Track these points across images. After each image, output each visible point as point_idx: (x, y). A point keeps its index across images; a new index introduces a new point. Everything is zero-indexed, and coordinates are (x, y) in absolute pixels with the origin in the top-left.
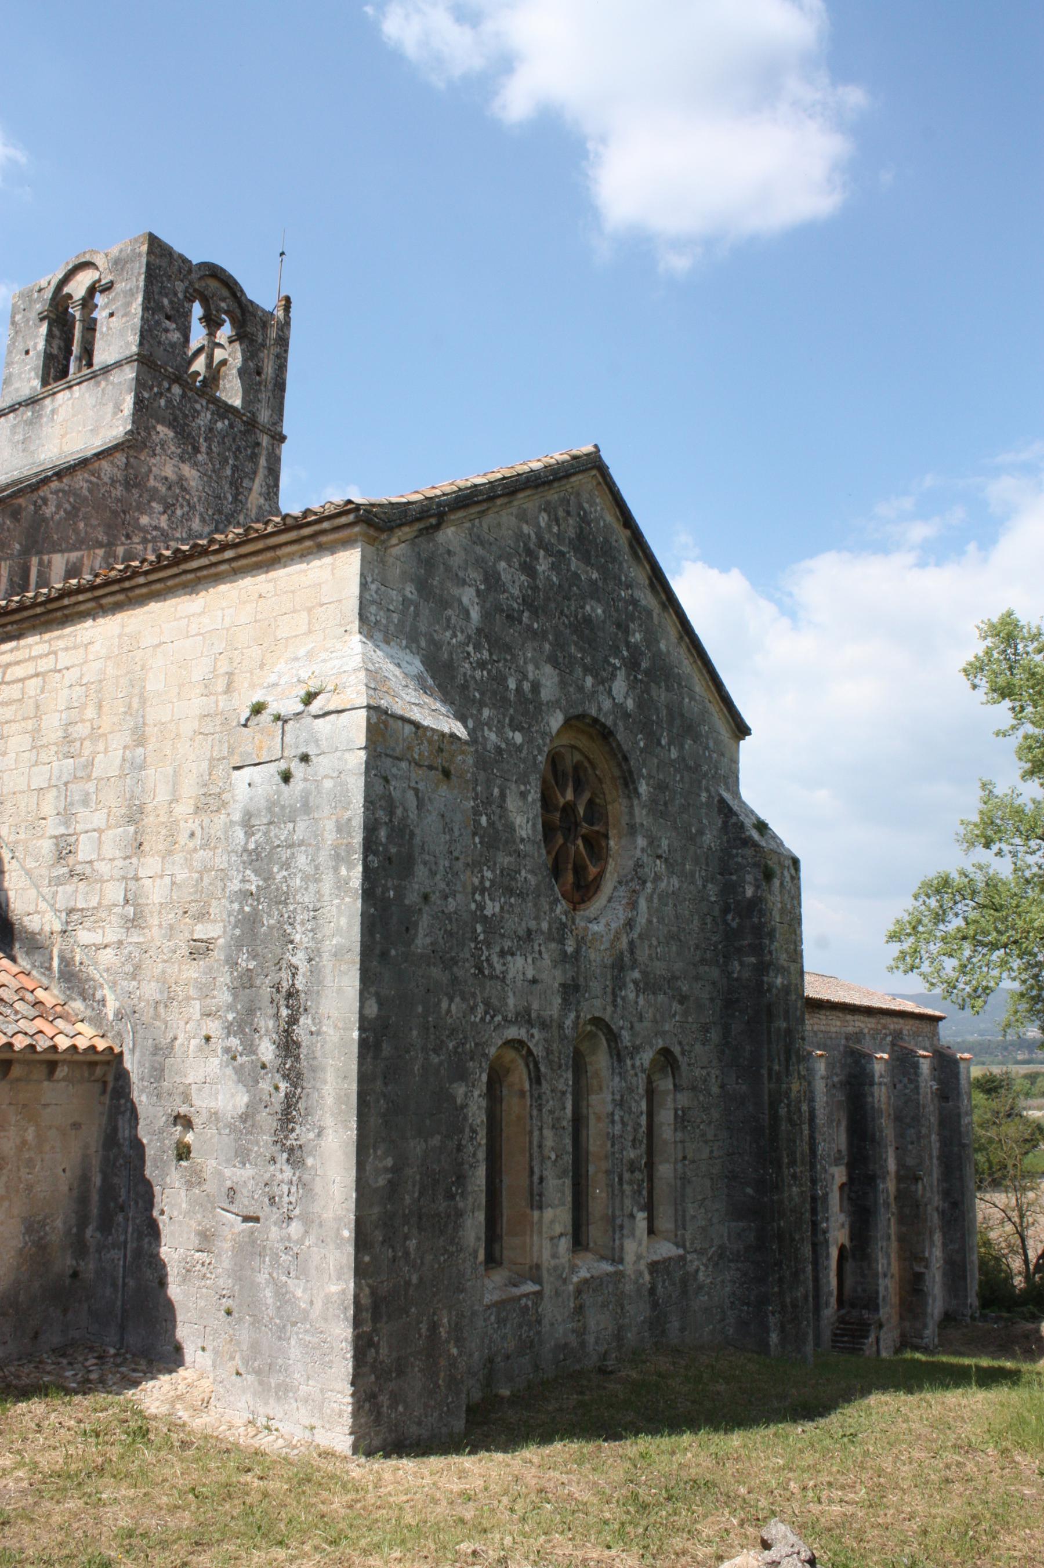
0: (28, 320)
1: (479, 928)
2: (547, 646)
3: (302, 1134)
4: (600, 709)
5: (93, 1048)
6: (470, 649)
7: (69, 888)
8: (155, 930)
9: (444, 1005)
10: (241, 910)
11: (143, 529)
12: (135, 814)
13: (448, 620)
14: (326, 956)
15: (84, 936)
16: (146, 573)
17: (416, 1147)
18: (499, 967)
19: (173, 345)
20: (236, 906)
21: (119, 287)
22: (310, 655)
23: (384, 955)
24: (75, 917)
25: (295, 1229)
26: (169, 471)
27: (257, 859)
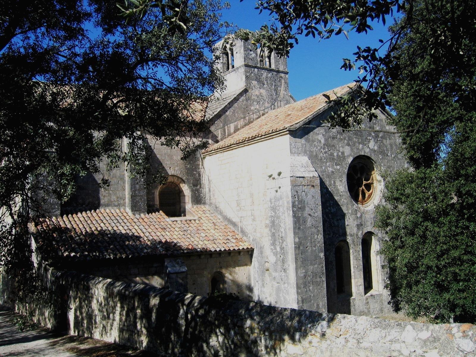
1: (330, 215)
2: (346, 141)
3: (286, 265)
4: (365, 152)
5: (248, 248)
6: (322, 150)
9: (316, 236)
11: (253, 111)
12: (252, 195)
13: (315, 145)
17: (312, 267)
18: (336, 223)
19: (253, 58)
23: (299, 228)
24: (242, 218)
25: (286, 285)
26: (257, 93)
27: (274, 209)
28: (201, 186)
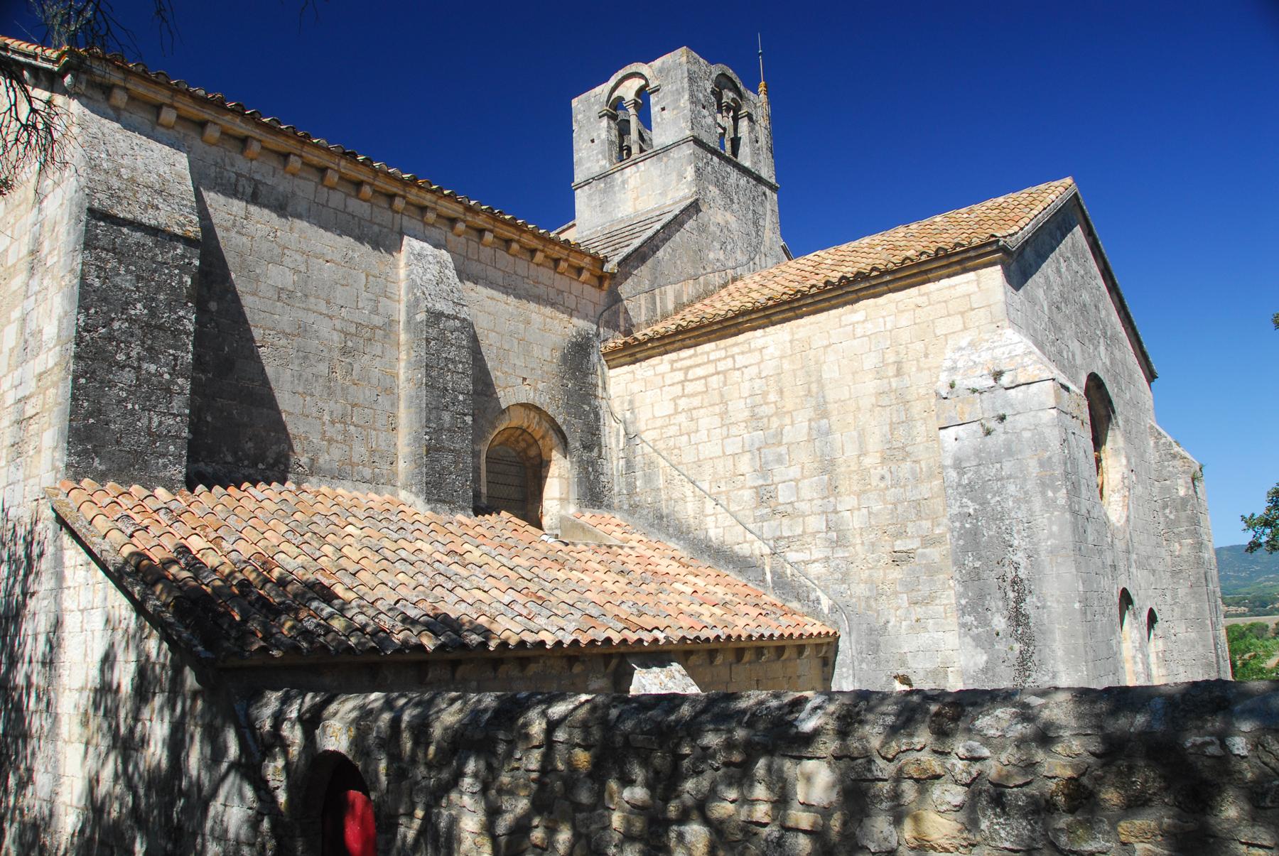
0: (589, 118)
7: (774, 523)
8: (858, 547)
10: (963, 527)
12: (827, 466)
14: (1043, 554)
15: (792, 556)
16: (813, 296)
20: (957, 524)
21: (665, 89)
22: (972, 344)
26: (720, 219)
28: (600, 452)
